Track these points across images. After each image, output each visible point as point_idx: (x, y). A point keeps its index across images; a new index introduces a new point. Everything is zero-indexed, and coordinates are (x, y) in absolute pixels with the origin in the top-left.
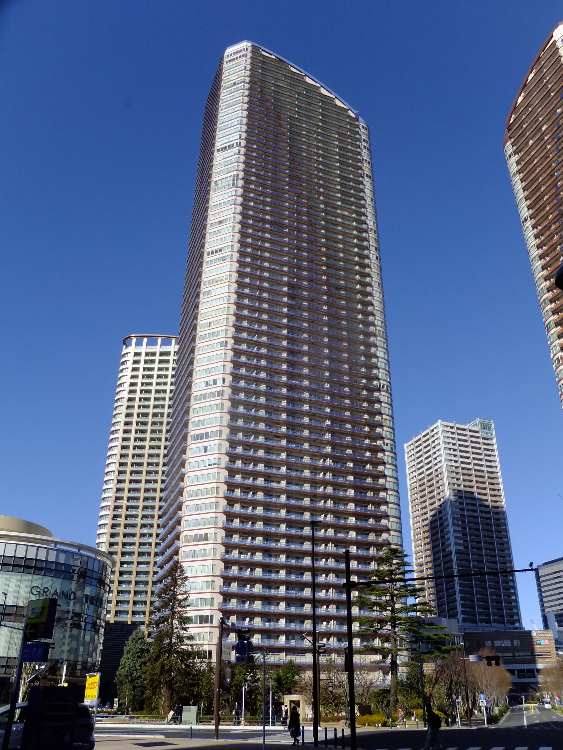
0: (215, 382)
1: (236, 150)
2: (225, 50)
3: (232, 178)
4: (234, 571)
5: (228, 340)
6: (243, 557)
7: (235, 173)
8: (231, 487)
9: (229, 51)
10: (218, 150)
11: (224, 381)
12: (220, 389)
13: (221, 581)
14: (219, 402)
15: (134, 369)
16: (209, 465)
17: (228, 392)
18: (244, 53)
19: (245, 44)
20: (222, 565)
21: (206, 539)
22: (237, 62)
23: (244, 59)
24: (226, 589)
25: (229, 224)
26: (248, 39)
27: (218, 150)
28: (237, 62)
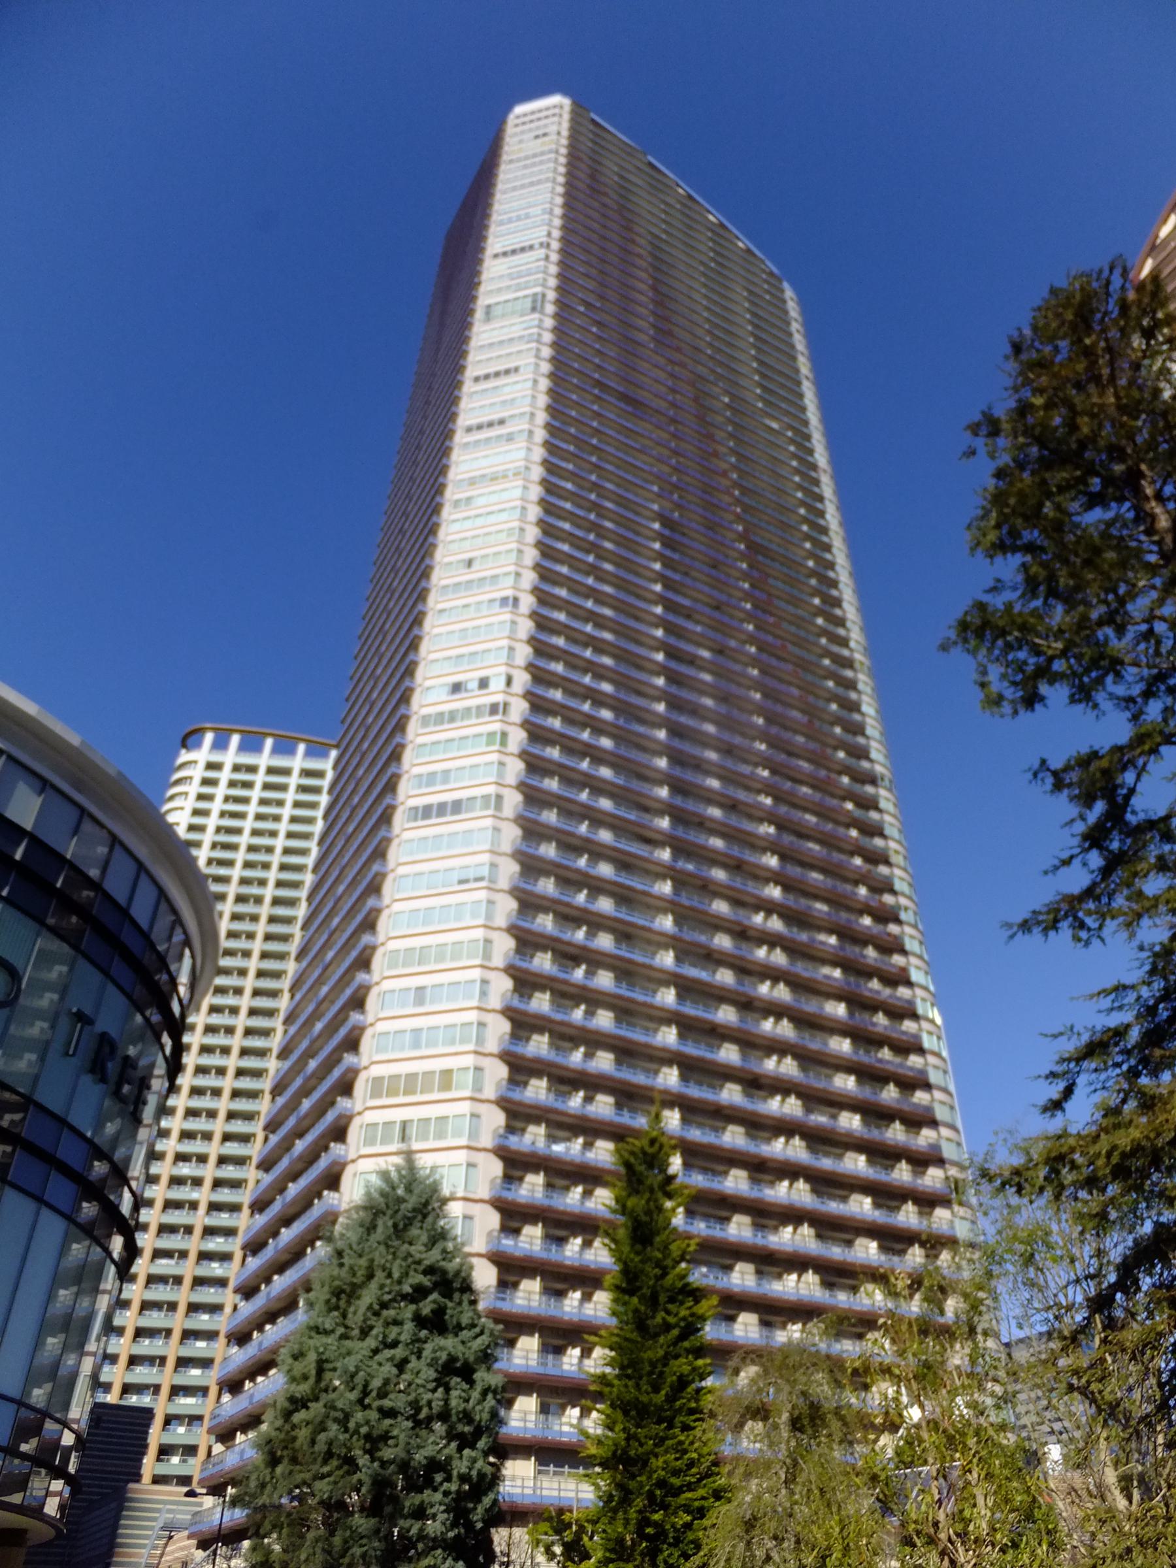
0: (484, 683)
1: (541, 253)
2: (509, 108)
3: (530, 300)
4: (533, 1187)
5: (519, 594)
6: (558, 1148)
7: (538, 289)
8: (527, 942)
9: (519, 109)
10: (496, 256)
11: (509, 681)
12: (499, 698)
13: (494, 1219)
14: (496, 727)
15: (206, 782)
16: (461, 882)
17: (519, 708)
18: (557, 111)
19: (556, 99)
20: (496, 1168)
21: (446, 1085)
22: (537, 137)
23: (556, 119)
24: (508, 1243)
25: (527, 374)
26: (565, 92)
27: (496, 256)
28: (537, 137)
